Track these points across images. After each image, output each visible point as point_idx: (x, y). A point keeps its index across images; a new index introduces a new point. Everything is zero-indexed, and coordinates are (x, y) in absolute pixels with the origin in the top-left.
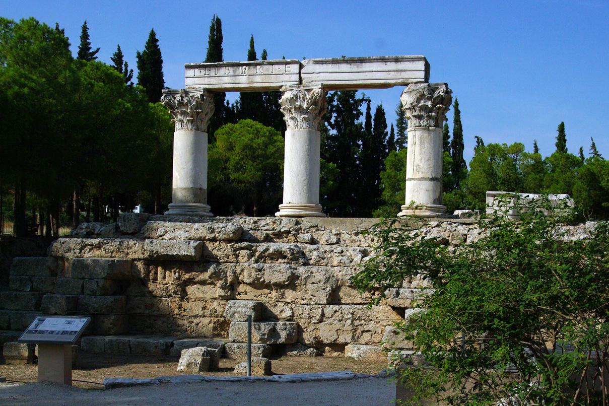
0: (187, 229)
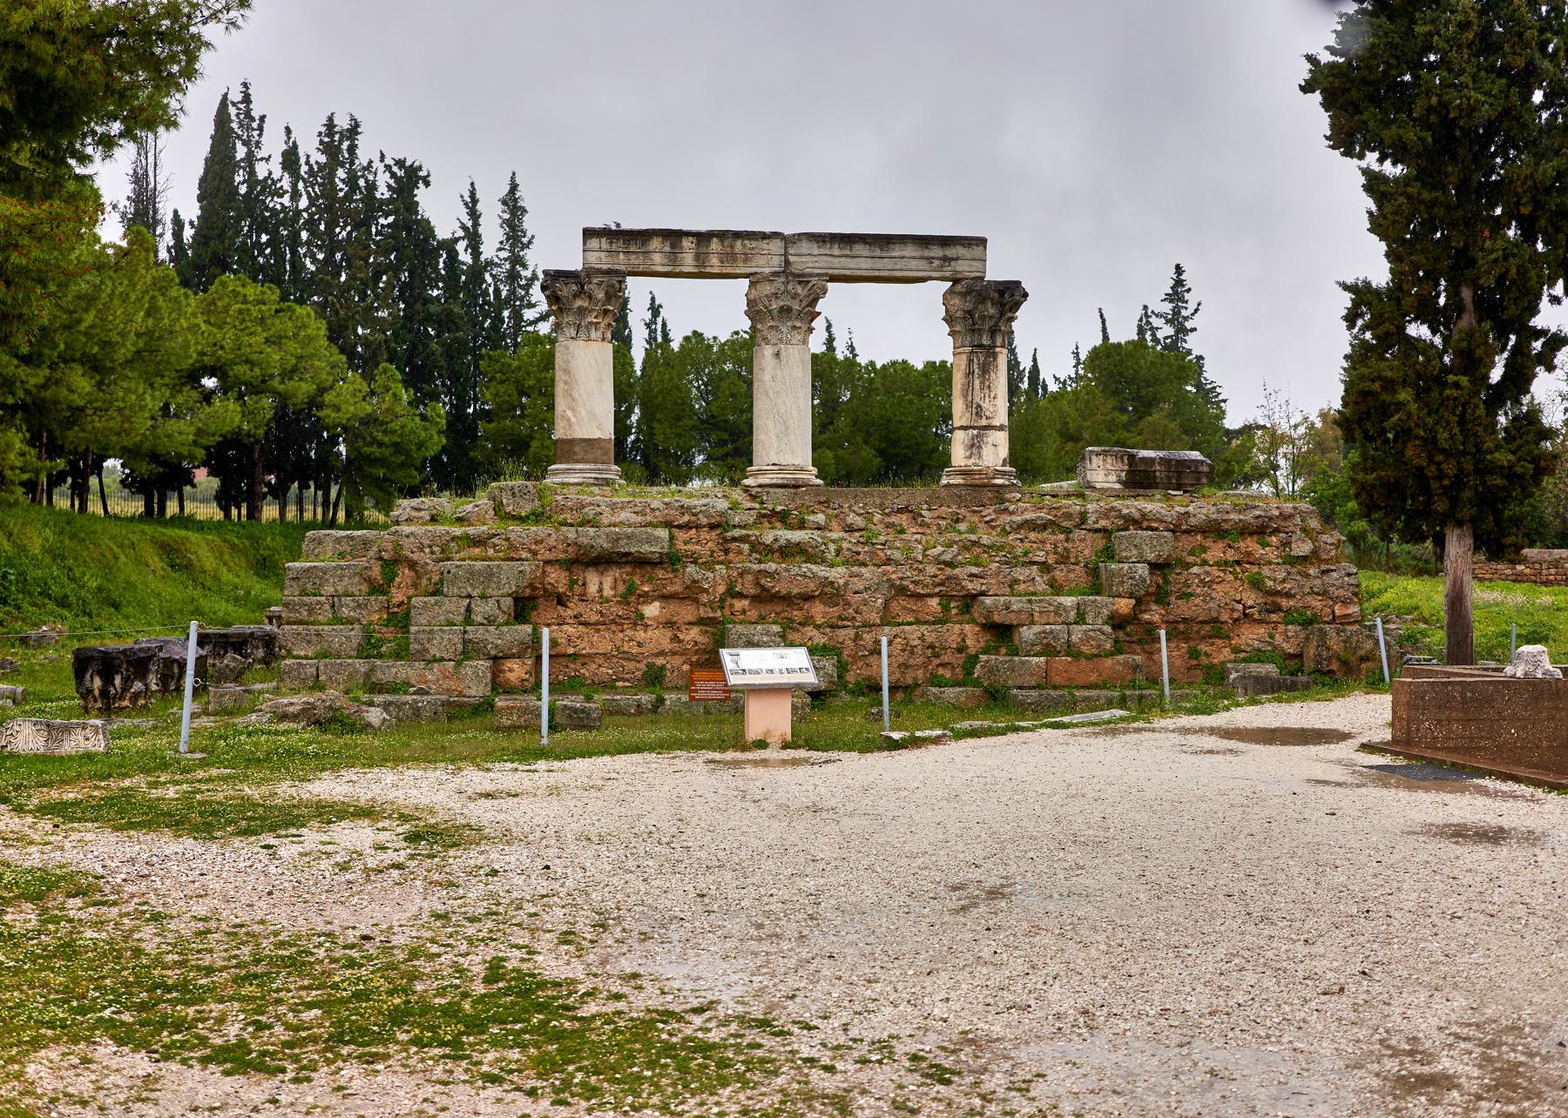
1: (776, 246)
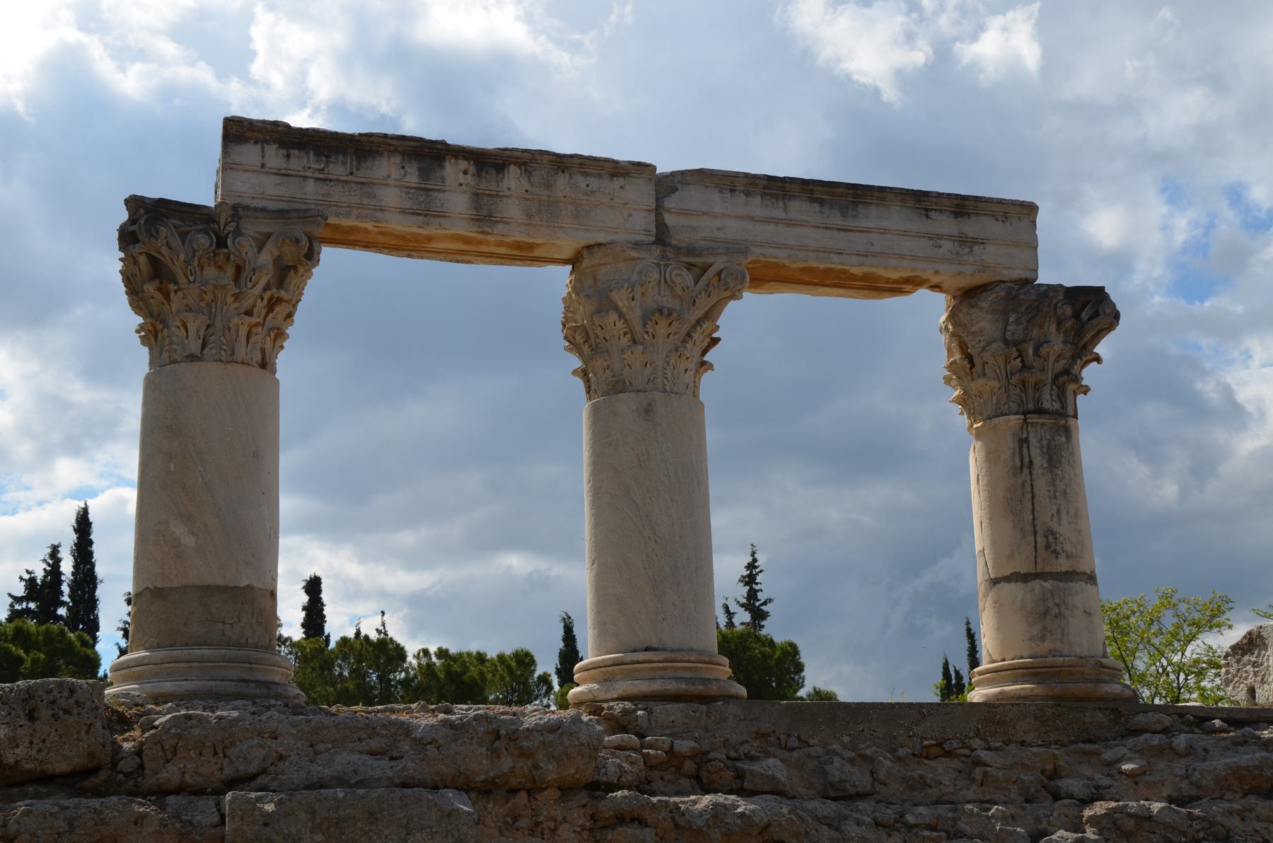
0: (376, 743)
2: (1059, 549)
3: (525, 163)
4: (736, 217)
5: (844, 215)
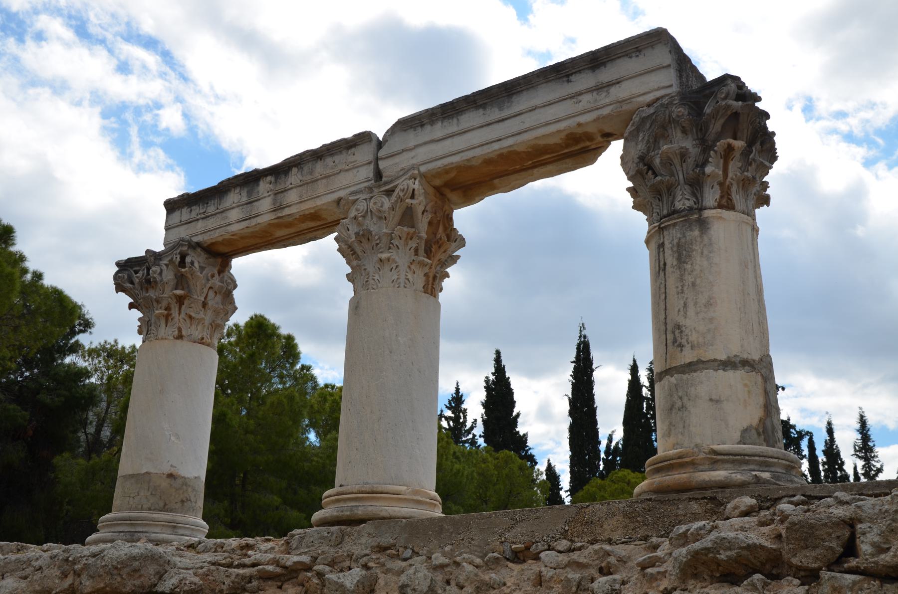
1: (364, 153)
2: (684, 342)
3: (299, 164)
4: (425, 143)
5: (501, 109)
